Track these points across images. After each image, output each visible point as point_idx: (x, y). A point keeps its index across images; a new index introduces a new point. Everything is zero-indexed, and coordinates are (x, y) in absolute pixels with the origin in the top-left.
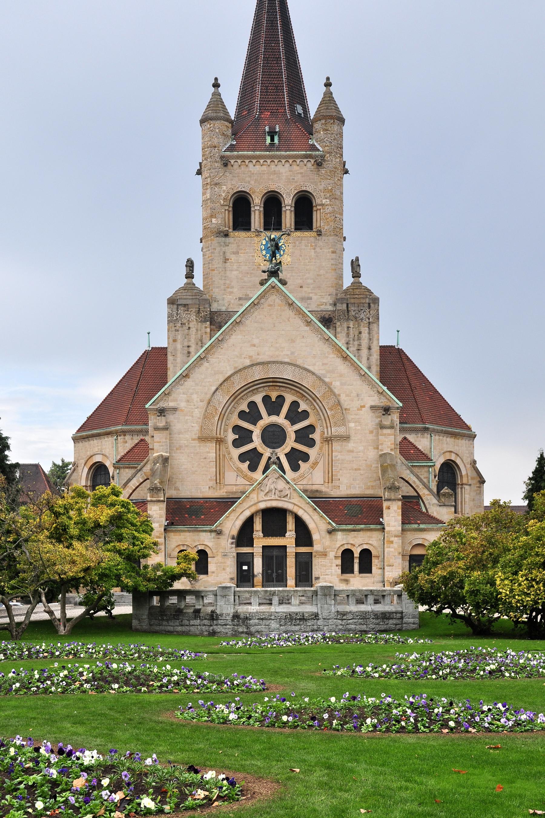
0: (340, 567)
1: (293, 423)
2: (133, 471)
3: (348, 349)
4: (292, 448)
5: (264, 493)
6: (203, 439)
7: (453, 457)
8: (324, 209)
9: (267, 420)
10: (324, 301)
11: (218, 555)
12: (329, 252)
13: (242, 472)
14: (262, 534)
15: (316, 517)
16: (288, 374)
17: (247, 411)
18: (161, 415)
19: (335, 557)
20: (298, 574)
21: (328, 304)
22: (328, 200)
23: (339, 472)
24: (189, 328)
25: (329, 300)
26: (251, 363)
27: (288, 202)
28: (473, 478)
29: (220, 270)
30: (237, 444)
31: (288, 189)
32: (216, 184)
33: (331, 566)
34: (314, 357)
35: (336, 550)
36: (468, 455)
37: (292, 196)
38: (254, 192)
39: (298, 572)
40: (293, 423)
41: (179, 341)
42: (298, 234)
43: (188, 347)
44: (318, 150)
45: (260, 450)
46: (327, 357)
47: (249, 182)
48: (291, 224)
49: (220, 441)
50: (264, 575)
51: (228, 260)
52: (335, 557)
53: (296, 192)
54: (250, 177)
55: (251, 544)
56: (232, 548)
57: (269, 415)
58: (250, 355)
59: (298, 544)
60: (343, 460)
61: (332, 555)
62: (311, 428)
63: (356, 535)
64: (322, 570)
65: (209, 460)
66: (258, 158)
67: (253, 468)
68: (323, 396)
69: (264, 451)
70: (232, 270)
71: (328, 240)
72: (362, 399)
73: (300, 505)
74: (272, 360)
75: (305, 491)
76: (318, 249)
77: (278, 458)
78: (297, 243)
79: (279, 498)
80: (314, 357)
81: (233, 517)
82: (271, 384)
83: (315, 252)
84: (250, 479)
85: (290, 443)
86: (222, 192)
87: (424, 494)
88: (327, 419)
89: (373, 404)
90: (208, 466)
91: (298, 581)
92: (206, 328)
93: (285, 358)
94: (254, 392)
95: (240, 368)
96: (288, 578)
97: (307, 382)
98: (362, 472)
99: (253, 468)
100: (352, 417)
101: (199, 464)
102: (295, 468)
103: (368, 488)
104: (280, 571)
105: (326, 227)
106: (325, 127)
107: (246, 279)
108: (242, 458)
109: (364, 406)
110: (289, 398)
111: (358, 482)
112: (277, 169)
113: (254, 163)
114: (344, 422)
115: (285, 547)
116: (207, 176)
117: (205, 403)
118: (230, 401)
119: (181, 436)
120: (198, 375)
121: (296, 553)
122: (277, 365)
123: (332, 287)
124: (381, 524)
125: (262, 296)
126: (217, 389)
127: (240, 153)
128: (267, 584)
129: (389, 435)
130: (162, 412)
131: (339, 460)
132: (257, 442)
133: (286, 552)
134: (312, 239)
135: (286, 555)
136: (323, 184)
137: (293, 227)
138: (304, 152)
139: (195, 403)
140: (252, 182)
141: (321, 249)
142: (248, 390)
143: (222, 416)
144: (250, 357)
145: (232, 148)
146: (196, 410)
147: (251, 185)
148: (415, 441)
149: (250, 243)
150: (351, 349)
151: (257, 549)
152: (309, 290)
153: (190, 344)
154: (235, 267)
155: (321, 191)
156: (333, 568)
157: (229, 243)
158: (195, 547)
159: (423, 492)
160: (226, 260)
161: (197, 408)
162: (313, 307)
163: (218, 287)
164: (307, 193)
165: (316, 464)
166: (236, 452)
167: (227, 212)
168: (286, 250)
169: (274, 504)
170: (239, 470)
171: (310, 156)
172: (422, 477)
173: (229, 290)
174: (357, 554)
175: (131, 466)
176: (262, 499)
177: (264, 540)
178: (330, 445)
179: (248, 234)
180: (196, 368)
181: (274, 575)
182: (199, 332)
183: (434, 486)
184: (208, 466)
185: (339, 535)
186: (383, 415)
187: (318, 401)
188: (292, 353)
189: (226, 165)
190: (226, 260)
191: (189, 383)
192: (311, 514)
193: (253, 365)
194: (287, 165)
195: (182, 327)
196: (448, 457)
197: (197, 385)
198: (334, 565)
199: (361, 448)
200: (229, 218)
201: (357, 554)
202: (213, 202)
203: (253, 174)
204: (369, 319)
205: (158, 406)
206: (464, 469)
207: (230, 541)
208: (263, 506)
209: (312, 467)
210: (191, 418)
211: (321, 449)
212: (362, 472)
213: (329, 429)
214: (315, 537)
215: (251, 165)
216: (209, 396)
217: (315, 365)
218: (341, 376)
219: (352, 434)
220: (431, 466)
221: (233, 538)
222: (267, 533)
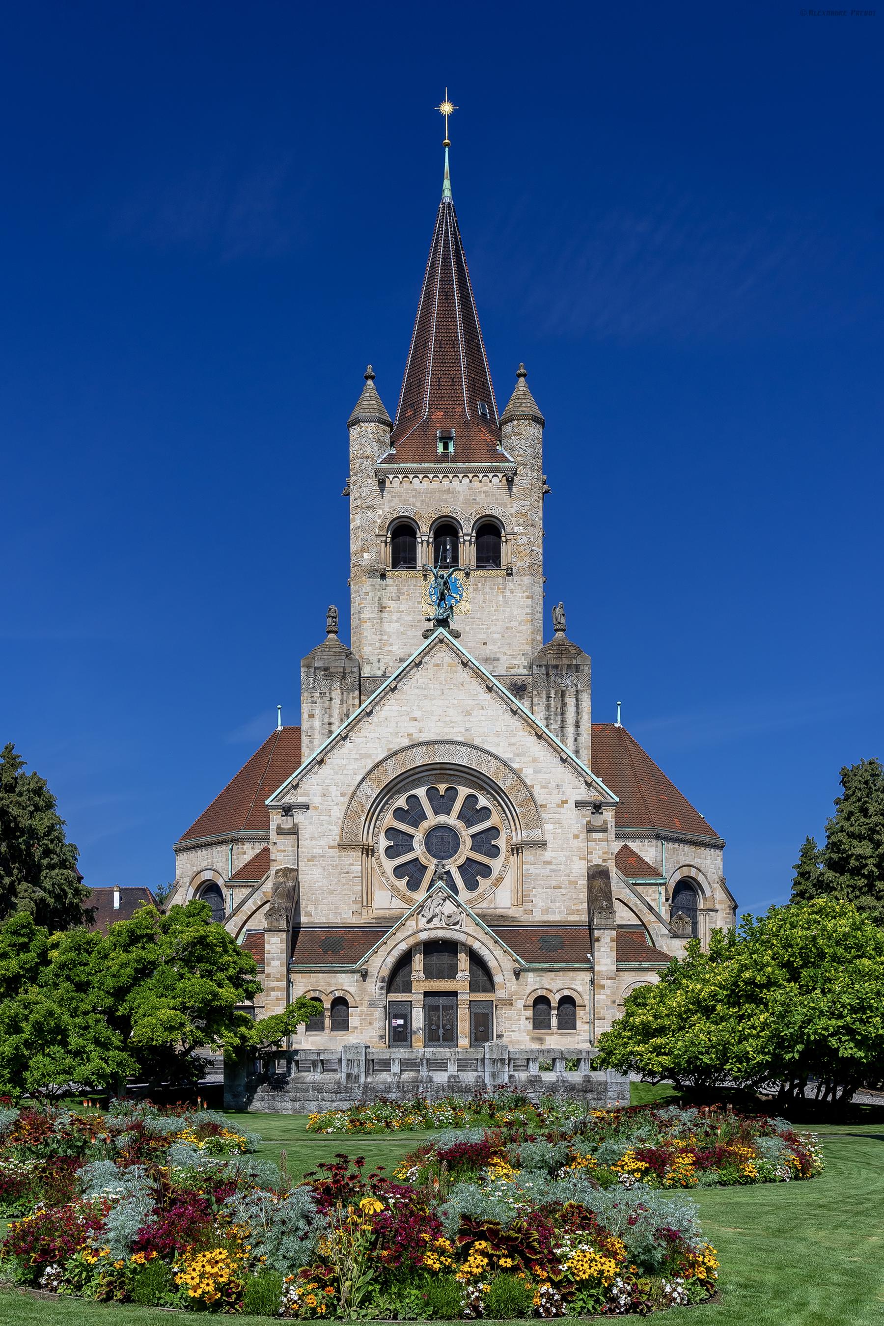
0: (532, 1021)
1: (469, 824)
2: (246, 891)
3: (547, 726)
5: (425, 920)
6: (343, 846)
7: (693, 873)
8: (515, 540)
9: (432, 820)
10: (516, 662)
13: (398, 890)
15: (498, 952)
16: (462, 757)
18: (286, 815)
21: (521, 667)
22: (521, 528)
24: (331, 699)
25: (523, 661)
26: (411, 743)
27: (467, 530)
28: (721, 902)
29: (375, 622)
30: (391, 852)
31: (467, 514)
32: (369, 507)
34: (497, 734)
36: (714, 871)
38: (421, 517)
40: (469, 824)
41: (317, 717)
42: (481, 573)
43: (330, 724)
44: (508, 461)
45: (423, 861)
46: (516, 735)
47: (414, 504)
48: (470, 560)
49: (369, 851)
50: (427, 1031)
51: (385, 608)
53: (478, 516)
54: (415, 497)
55: (407, 988)
56: (382, 994)
57: (436, 813)
58: (410, 732)
59: (473, 989)
60: (536, 875)
61: (520, 1004)
62: (494, 831)
63: (553, 977)
65: (353, 875)
66: (425, 473)
67: (414, 886)
68: (511, 788)
69: (428, 863)
70: (391, 622)
72: (563, 792)
73: (476, 936)
74: (439, 738)
75: (483, 917)
76: (508, 593)
77: (448, 873)
78: (480, 585)
80: (497, 734)
81: (383, 951)
82: (438, 772)
83: (504, 597)
84: (409, 901)
85: (465, 851)
86: (377, 516)
87: (649, 921)
88: (516, 818)
89: (579, 798)
90: (351, 883)
91: (473, 1039)
92: (354, 698)
93: (457, 736)
94: (416, 784)
95: (394, 750)
97: (488, 769)
98: (563, 891)
99: (414, 886)
100: (550, 816)
101: (339, 881)
102: (472, 885)
103: (572, 913)
105: (519, 564)
107: (409, 633)
108: (399, 871)
109: (566, 802)
110: (463, 791)
111: (557, 904)
112: (451, 486)
113: (421, 478)
114: (538, 822)
115: (455, 994)
116: (356, 496)
117: (347, 799)
119: (314, 842)
120: (336, 759)
121: (470, 1001)
122: (447, 746)
123: (527, 643)
124: (588, 961)
125: (426, 652)
126: (363, 779)
127: (402, 465)
128: (431, 1043)
129: (601, 840)
130: (287, 810)
132: (419, 850)
134: (500, 580)
136: (515, 505)
137: (474, 563)
138: (489, 464)
139: (334, 798)
140: (418, 505)
142: (407, 781)
143: (370, 815)
144: (410, 735)
145: (390, 459)
147: (416, 507)
148: (641, 851)
149: (415, 586)
150: (553, 727)
151: (416, 996)
152: (495, 649)
153: (332, 720)
154: (394, 618)
155: (512, 514)
157: (387, 586)
158: (331, 992)
159: (648, 918)
160: (382, 609)
161: (337, 804)
162: (501, 671)
163: (370, 645)
164: (492, 519)
165: (499, 880)
166: (389, 865)
167: (383, 544)
168: (464, 594)
169: (440, 934)
170: (393, 888)
171: (496, 470)
172: (648, 899)
173: (387, 648)
174: (554, 1004)
175: (250, 884)
177: (426, 983)
178: (520, 854)
179: (412, 573)
180: (335, 751)
181: (441, 1031)
182: (345, 704)
183: (664, 911)
185: (531, 977)
186: (593, 813)
188: (467, 730)
189: (382, 483)
190: (382, 609)
191: (325, 771)
192: (491, 947)
193: (413, 746)
194: (466, 481)
195: (321, 698)
196: (685, 872)
197: (336, 773)
198: (523, 1018)
199: (563, 859)
200: (387, 552)
201: (554, 1004)
202: (364, 531)
203: (419, 493)
204: (577, 686)
205: (283, 801)
206: (709, 889)
207: (379, 984)
208: (424, 936)
209: (495, 885)
210: (327, 818)
212: (563, 891)
213: (519, 832)
214: (498, 979)
215: (416, 481)
216: (352, 788)
217: (498, 745)
218: (535, 760)
219: (549, 838)
220: (661, 884)
222: (430, 973)
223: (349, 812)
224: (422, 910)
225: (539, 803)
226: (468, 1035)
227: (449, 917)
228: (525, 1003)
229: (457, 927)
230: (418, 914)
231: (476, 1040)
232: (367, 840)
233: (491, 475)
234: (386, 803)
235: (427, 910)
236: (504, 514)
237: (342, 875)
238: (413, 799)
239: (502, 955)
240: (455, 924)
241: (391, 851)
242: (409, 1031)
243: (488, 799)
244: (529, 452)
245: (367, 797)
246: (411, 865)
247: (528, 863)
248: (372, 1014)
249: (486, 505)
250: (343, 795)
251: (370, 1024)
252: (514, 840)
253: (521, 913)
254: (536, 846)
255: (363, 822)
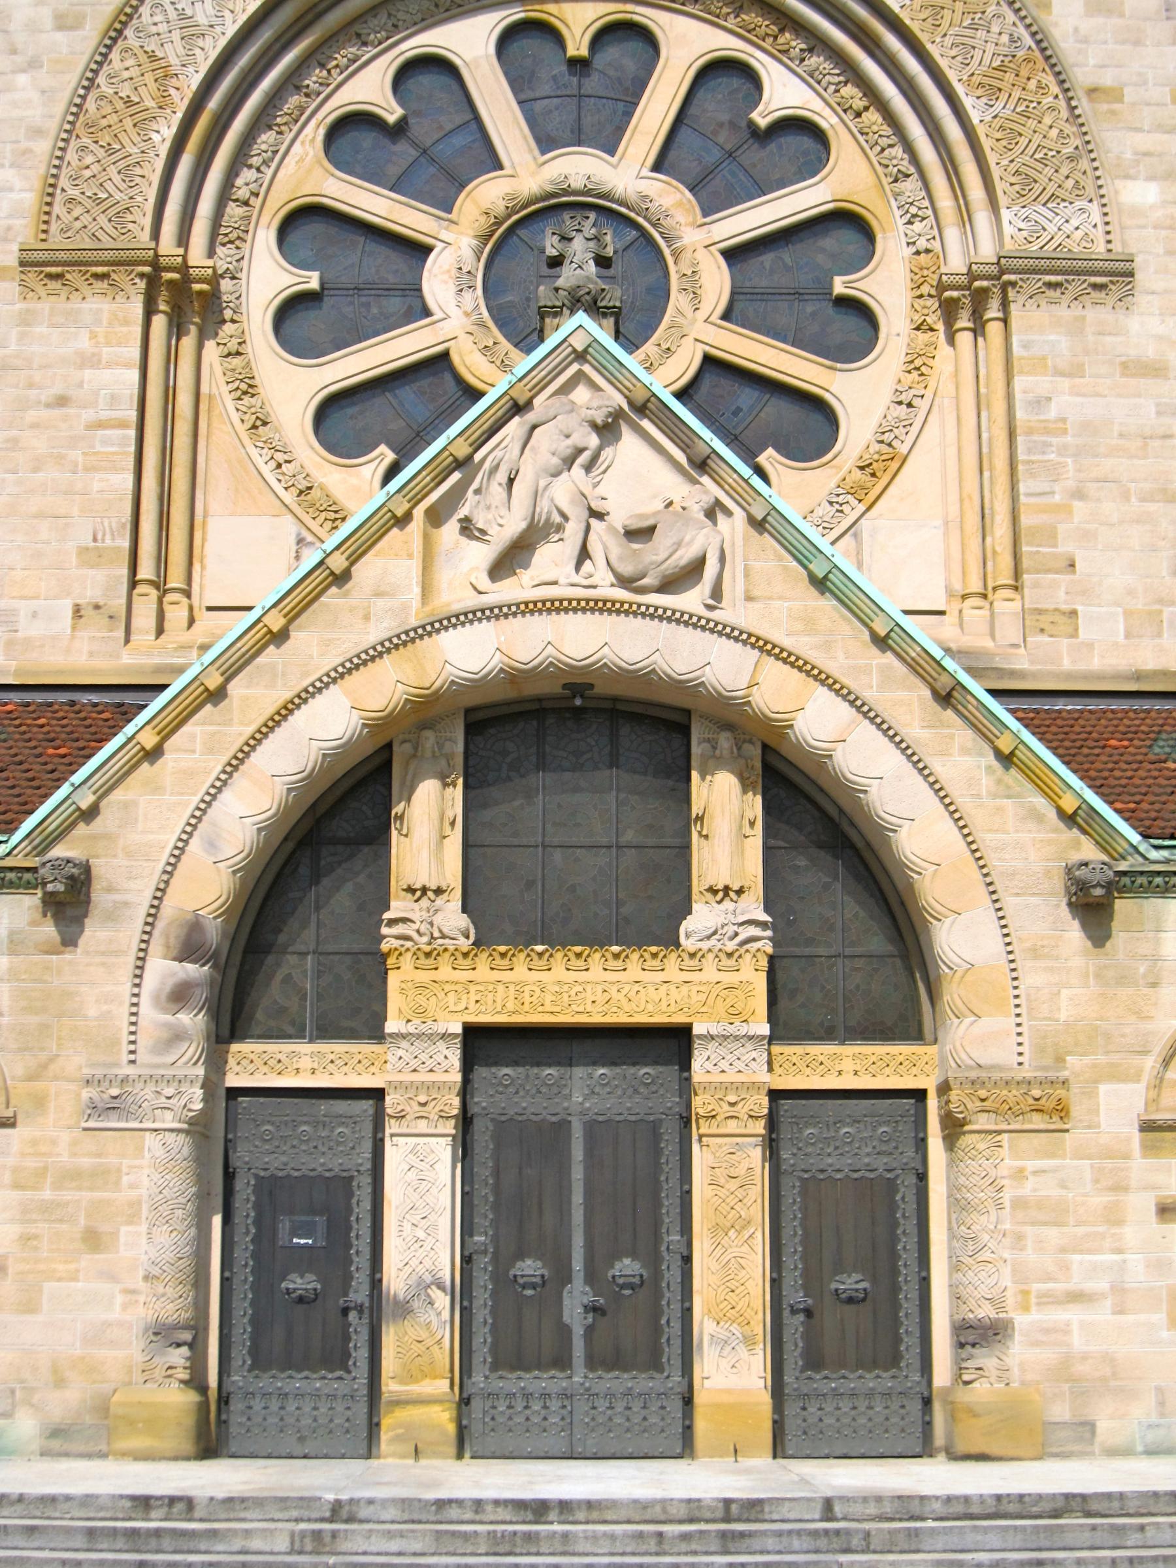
4: (709, 361)
5: (480, 555)
11: (40, 1102)
14: (464, 921)
17: (392, 113)
19: (1148, 1127)
20: (795, 1296)
23: (1064, 510)
33: (1114, 1217)
35: (1150, 1063)
39: (792, 1279)
50: (482, 1297)
52: (1148, 1127)
56: (177, 1036)
57: (546, 142)
64: (1030, 1256)
65: (88, 415)
79: (621, 594)
90: (76, 455)
96: (704, 1325)
100: (1143, 141)
101: (14, 444)
104: (627, 1267)
118: (266, 35)
121: (775, 1095)
131: (1060, 426)
133: (686, 1088)
135: (686, 1121)
146: (22, 79)
156: (1130, 1234)
161: (33, 64)
176: (472, 601)
178: (994, 329)
184: (76, 455)
187: (892, 42)
198: (1146, 1204)
209: (857, 491)
211: (917, 365)
221: (189, 950)
223: (90, 105)
224: (456, 496)
225: (1082, 75)
226: (759, 1320)
227: (640, 534)
228: (1153, 1102)
229: (691, 600)
230: (436, 517)
231: (814, 1361)
232: (183, 238)
234: (291, 82)
235: (496, 490)
237: (32, 415)
238: (425, 81)
239: (986, 783)
240: (671, 584)
241: (307, 322)
242: (359, 1293)
243: (812, 79)
245: (192, 34)
246: (406, 393)
247: (1040, 365)
248: (102, 1176)
250: (63, 23)
251: (94, 1240)
252: (956, 263)
253: (1010, 632)
254: (1077, 285)
255: (164, 150)
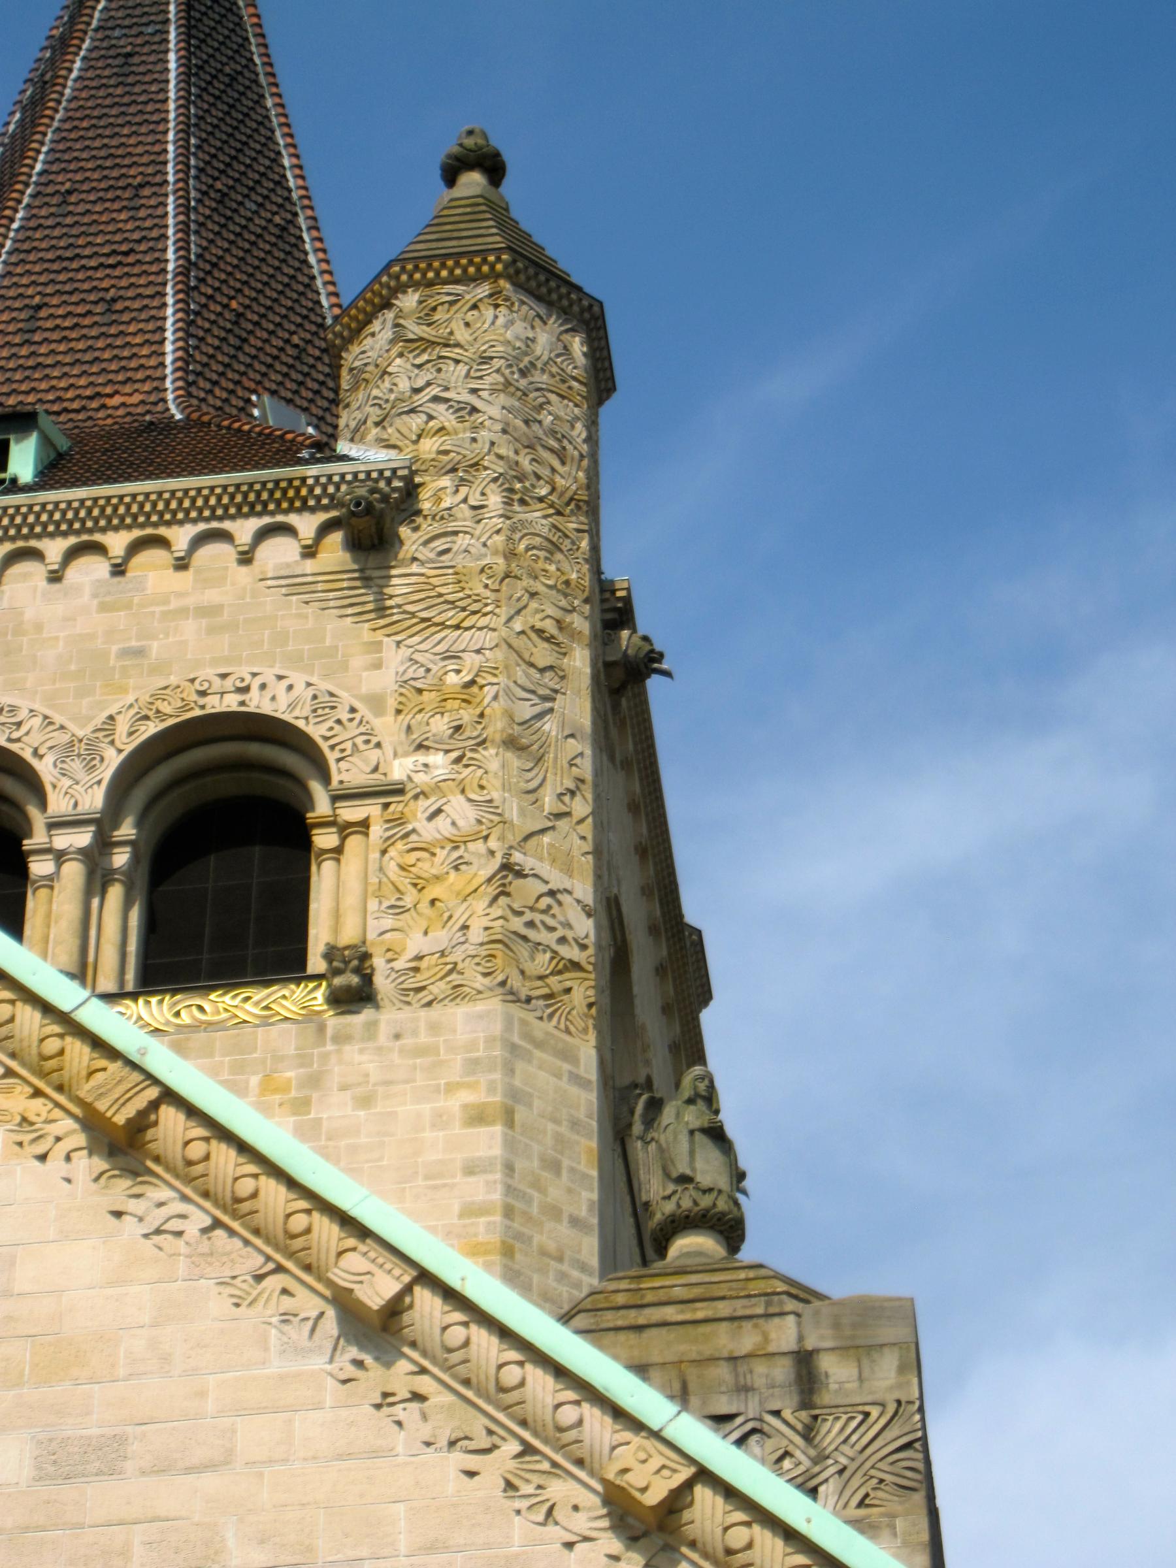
12: (439, 1120)
22: (439, 761)
37: (113, 760)
53: (152, 728)
71: (434, 1028)
105: (415, 943)
106: (414, 329)
134: (285, 1040)
141: (365, 1101)
155: (376, 702)
194: (92, 569)
233: (245, 529)
236: (323, 704)
244: (495, 411)
249: (209, 673)
